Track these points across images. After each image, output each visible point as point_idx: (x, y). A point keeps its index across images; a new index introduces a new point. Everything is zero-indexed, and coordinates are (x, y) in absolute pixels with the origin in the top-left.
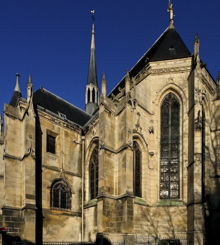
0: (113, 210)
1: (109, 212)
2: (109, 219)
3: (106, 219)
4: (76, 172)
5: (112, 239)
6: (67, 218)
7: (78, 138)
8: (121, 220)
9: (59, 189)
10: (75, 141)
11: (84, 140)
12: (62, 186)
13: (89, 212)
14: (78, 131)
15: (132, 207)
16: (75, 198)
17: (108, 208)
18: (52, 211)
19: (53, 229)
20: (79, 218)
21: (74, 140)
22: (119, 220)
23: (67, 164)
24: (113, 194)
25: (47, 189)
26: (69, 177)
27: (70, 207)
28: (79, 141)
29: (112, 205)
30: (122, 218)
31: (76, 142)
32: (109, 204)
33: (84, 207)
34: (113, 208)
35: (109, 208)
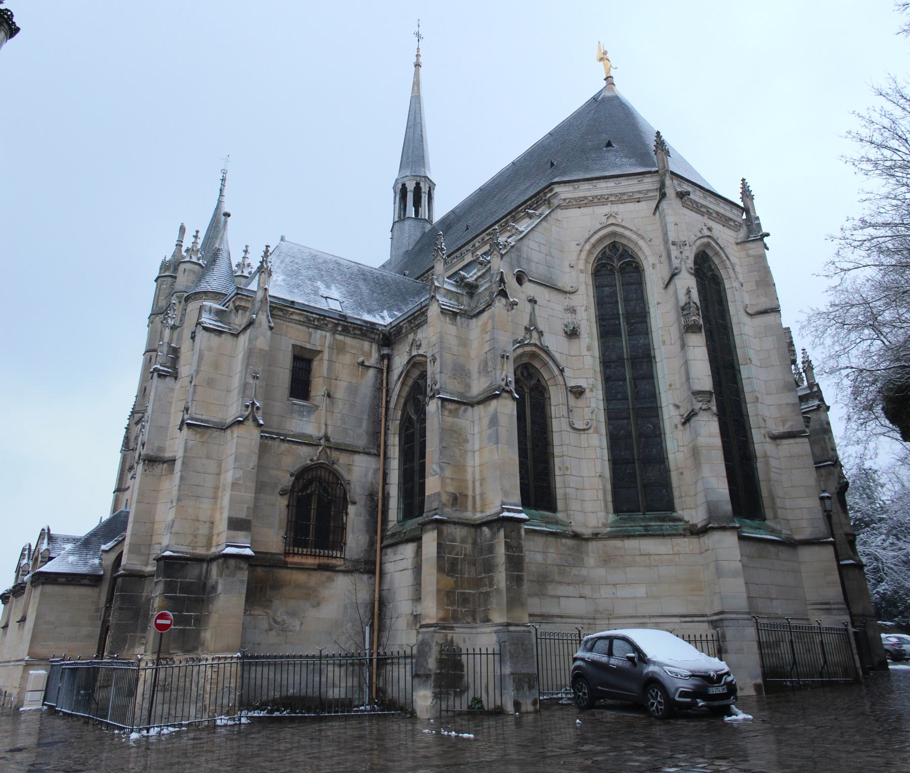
0: (465, 555)
1: (454, 563)
3: (449, 581)
4: (361, 442)
5: (464, 642)
6: (331, 580)
7: (371, 354)
8: (491, 585)
9: (310, 495)
10: (363, 362)
11: (389, 357)
12: (321, 483)
13: (399, 557)
14: (373, 336)
15: (520, 548)
16: (358, 515)
18: (290, 559)
19: (288, 613)
20: (365, 577)
21: (360, 360)
22: (485, 585)
23: (339, 422)
24: (466, 509)
25: (279, 497)
26: (343, 459)
27: (339, 544)
28: (373, 360)
29: (463, 541)
30: (491, 580)
31: (367, 363)
32: (454, 541)
33: (382, 543)
34: (465, 549)
35: (455, 552)
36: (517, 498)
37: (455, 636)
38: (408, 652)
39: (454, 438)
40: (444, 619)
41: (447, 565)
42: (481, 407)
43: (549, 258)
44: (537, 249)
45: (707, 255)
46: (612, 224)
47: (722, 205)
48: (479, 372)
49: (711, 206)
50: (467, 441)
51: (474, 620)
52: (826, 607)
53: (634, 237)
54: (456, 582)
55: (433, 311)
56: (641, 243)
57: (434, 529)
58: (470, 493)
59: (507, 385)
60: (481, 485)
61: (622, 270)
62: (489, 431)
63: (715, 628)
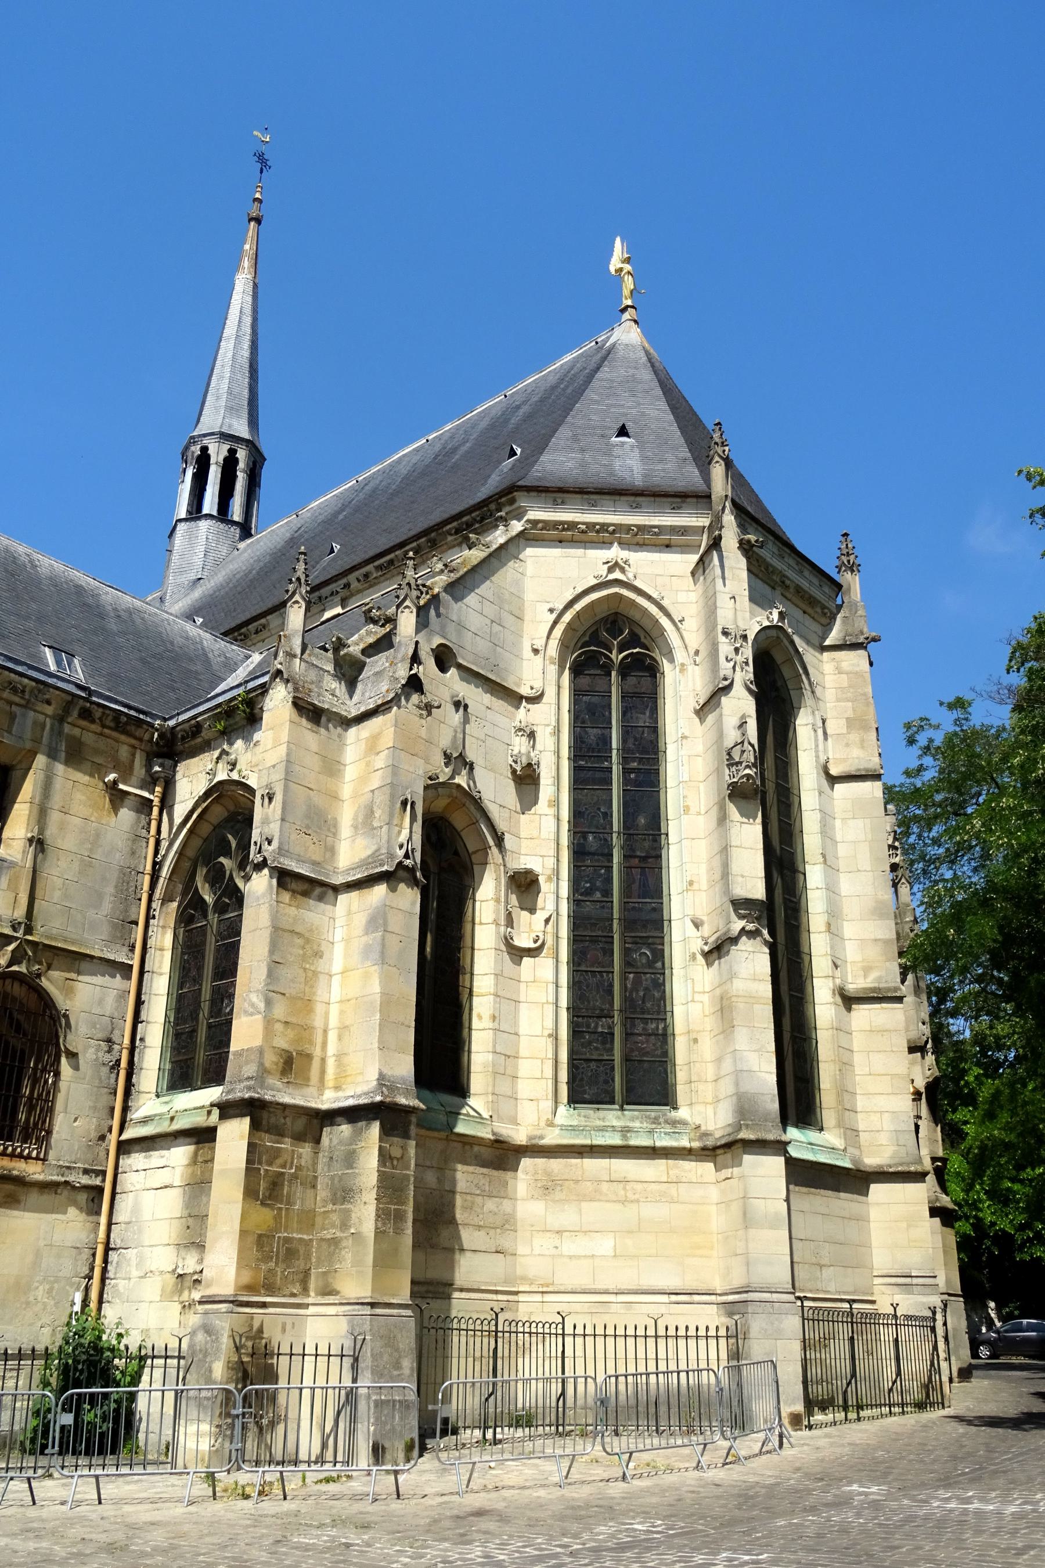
0: (299, 1168)
2: (275, 1218)
5: (284, 1330)
8: (345, 1225)
17: (276, 1158)
22: (333, 1226)
24: (306, 1082)
30: (347, 1213)
34: (300, 1157)
35: (279, 1161)
36: (404, 1067)
37: (266, 1318)
38: (173, 1344)
39: (297, 951)
40: (250, 1288)
41: (263, 1185)
42: (354, 895)
43: (496, 628)
44: (477, 607)
45: (773, 660)
46: (617, 582)
47: (806, 573)
48: (355, 827)
49: (790, 573)
50: (318, 954)
51: (305, 1291)
52: (904, 1280)
53: (653, 610)
54: (277, 1218)
55: (278, 703)
56: (664, 622)
57: (243, 1115)
58: (317, 1052)
59: (407, 856)
60: (340, 1038)
61: (625, 670)
62: (364, 939)
63: (730, 1314)
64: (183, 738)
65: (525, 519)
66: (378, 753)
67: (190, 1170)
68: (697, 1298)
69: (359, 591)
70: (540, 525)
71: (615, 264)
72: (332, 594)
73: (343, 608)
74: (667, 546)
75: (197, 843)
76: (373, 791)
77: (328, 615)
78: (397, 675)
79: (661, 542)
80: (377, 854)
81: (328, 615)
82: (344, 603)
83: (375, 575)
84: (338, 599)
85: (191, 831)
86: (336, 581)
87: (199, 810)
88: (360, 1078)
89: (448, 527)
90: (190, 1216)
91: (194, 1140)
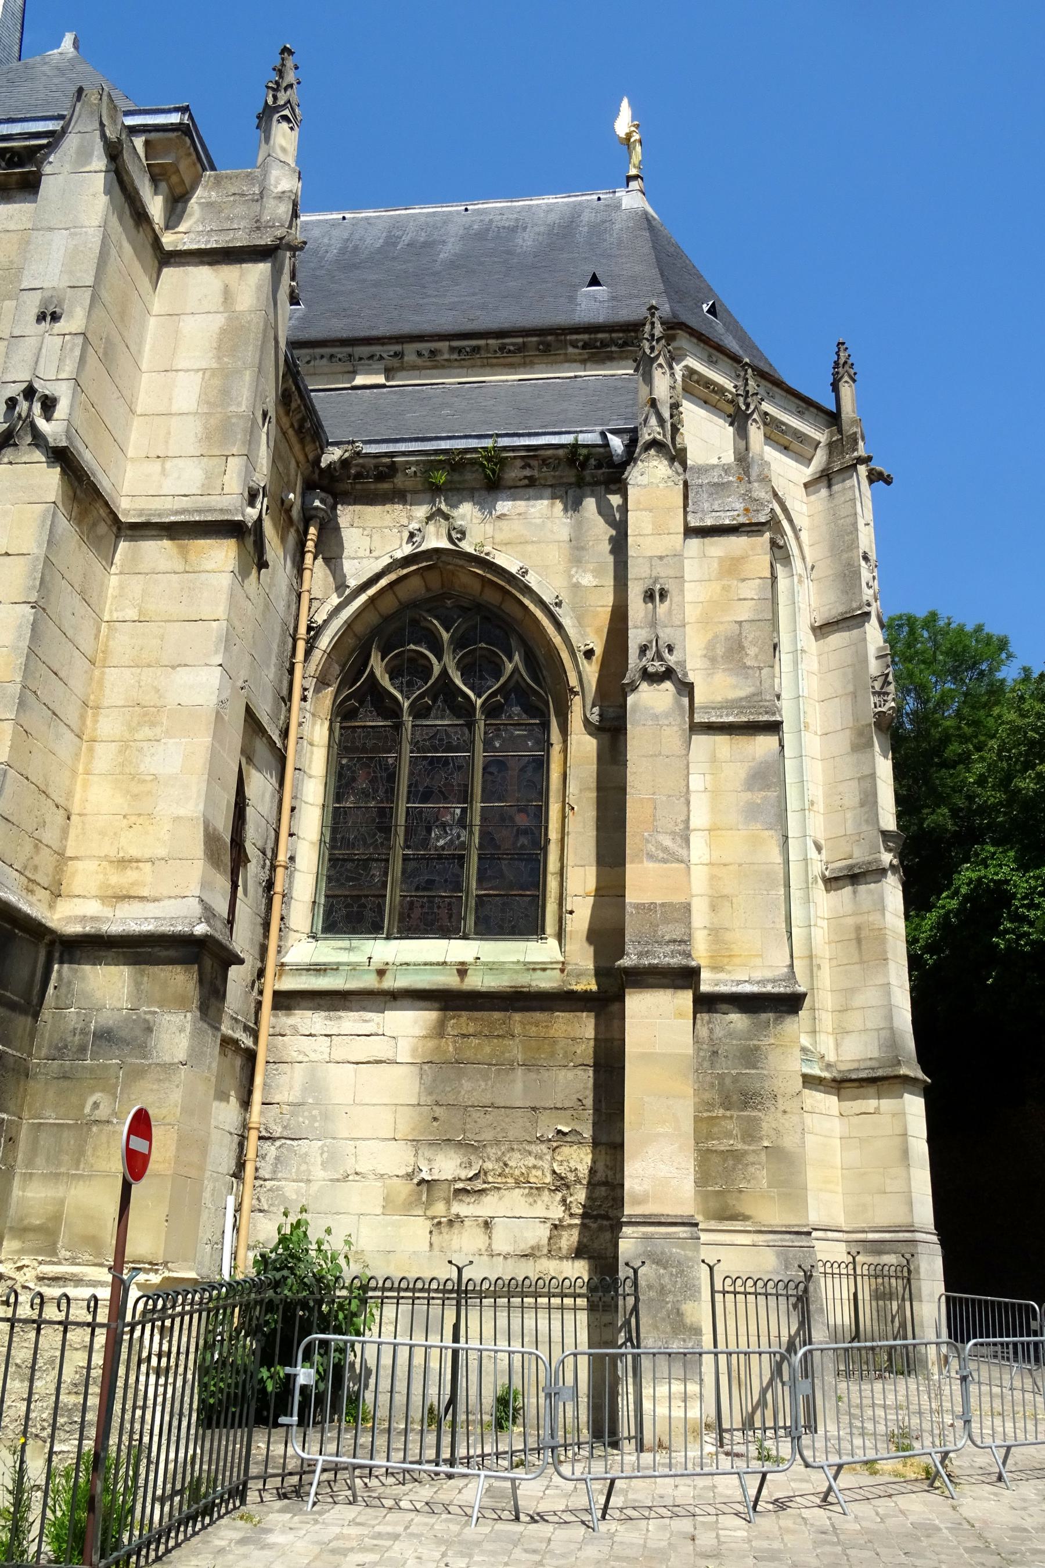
22: (729, 1135)
62: (749, 795)
64: (359, 476)
65: (684, 363)
66: (744, 580)
67: (431, 1044)
68: (830, 1235)
69: (414, 368)
70: (695, 377)
71: (623, 124)
72: (371, 357)
73: (387, 379)
74: (786, 448)
75: (372, 618)
76: (740, 623)
77: (360, 380)
78: (755, 495)
79: (782, 441)
80: (756, 698)
81: (360, 380)
82: (389, 373)
83: (446, 356)
84: (381, 366)
85: (372, 600)
86: (383, 344)
87: (392, 577)
88: (758, 961)
89: (575, 337)
90: (437, 1104)
91: (437, 1005)
